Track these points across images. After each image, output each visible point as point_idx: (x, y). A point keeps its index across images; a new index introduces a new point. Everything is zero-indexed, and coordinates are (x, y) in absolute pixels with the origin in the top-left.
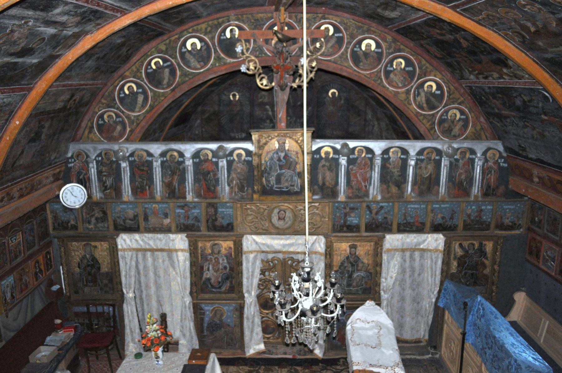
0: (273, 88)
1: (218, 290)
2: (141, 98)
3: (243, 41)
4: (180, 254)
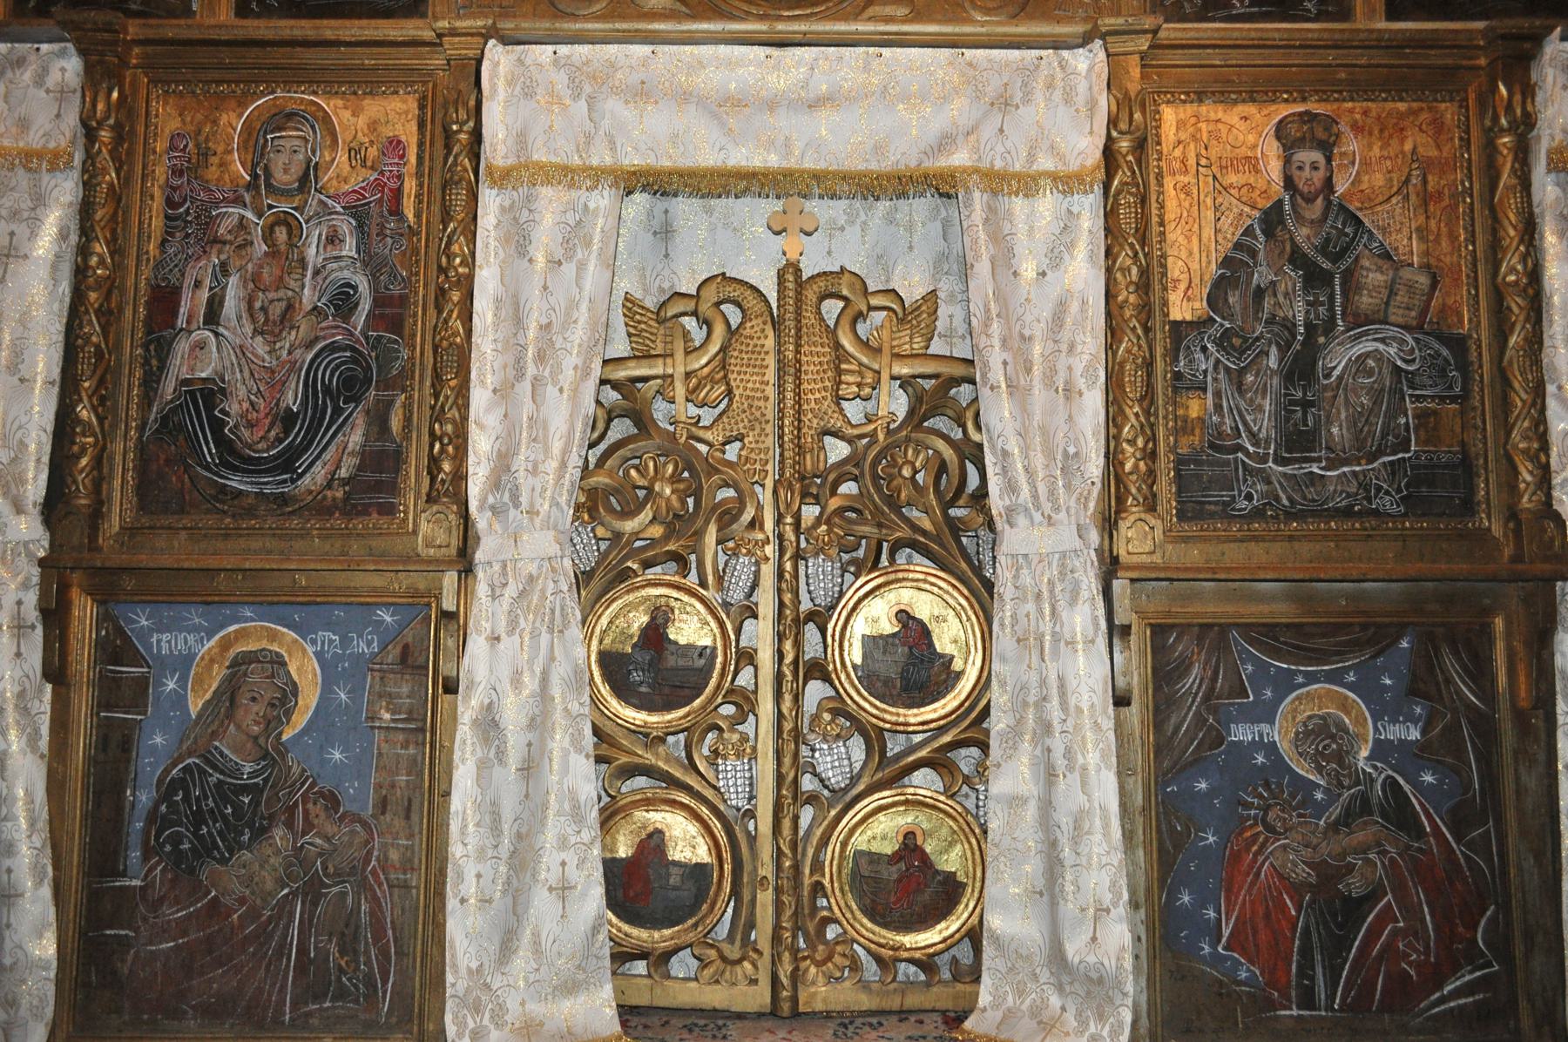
1: (271, 485)
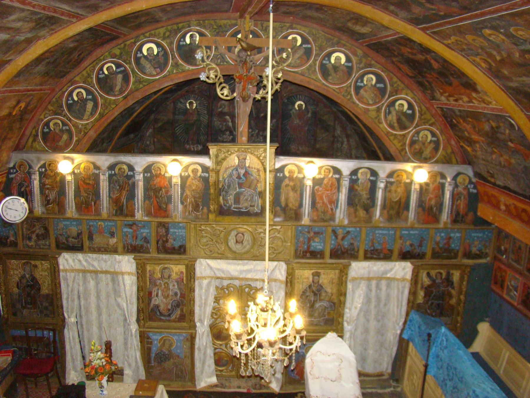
0: (235, 98)
1: (167, 318)
2: (90, 106)
3: (204, 48)
4: (126, 277)
